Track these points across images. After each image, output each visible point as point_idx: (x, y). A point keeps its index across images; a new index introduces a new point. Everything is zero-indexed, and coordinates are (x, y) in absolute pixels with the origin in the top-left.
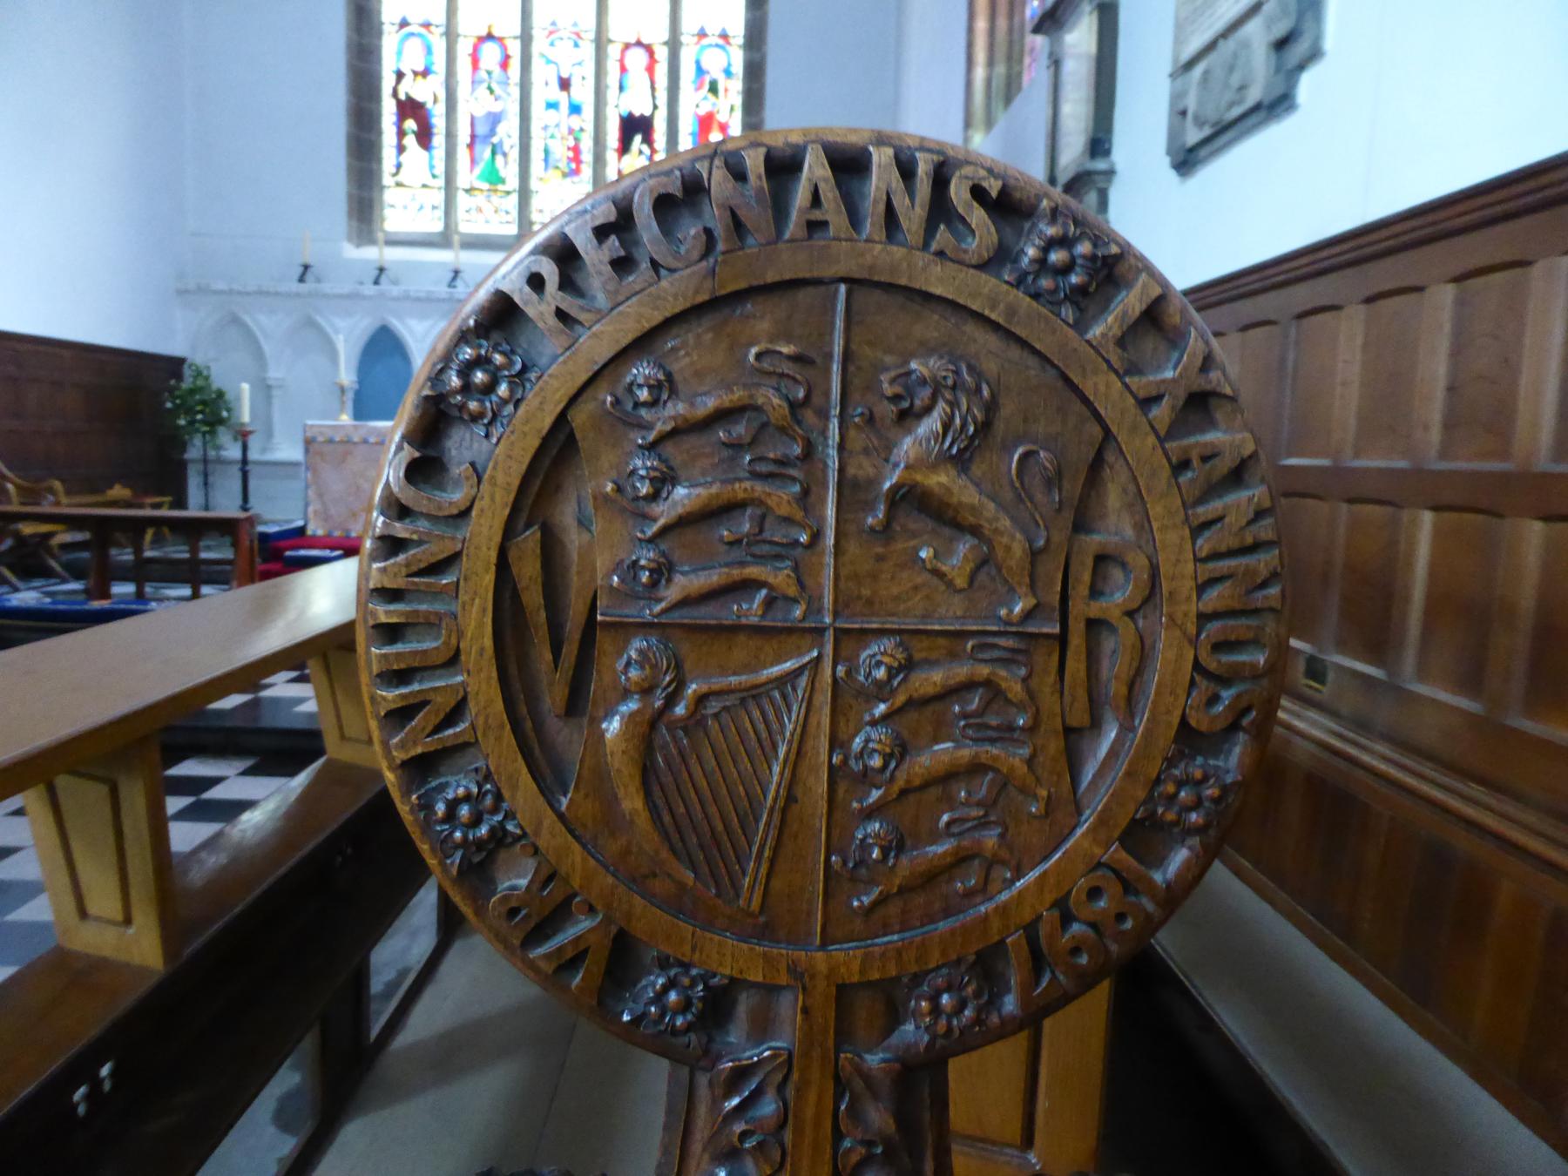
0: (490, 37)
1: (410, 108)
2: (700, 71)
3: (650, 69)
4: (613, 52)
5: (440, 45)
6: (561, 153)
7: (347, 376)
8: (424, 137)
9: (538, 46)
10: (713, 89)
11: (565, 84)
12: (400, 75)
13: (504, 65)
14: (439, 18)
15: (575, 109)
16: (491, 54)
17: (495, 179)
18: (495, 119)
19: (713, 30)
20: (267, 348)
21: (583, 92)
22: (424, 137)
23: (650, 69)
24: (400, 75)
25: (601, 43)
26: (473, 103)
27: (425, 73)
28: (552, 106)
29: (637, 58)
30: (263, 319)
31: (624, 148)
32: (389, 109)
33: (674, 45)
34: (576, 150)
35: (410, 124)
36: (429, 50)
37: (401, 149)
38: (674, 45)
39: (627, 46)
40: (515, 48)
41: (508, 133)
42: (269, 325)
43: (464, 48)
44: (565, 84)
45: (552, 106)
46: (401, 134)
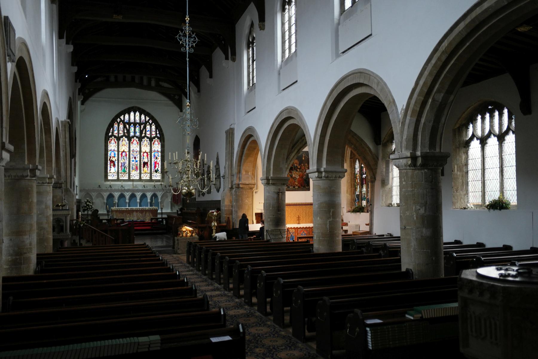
0: (124, 151)
1: (112, 162)
2: (154, 156)
3: (147, 156)
4: (142, 153)
5: (116, 153)
6: (134, 167)
7: (105, 201)
8: (114, 165)
9: (131, 152)
10: (157, 158)
11: (135, 158)
12: (110, 157)
13: (126, 155)
14: (116, 149)
15: (137, 161)
16: (124, 154)
17: (125, 171)
18: (124, 163)
19: (156, 150)
20: (93, 197)
21: (138, 159)
22: (114, 165)
23: (147, 156)
24: (110, 157)
25: (140, 151)
26: (121, 161)
27: (114, 157)
28: (133, 161)
29: (145, 154)
30: (93, 193)
31: (144, 167)
32: (109, 161)
33: (151, 152)
34: (137, 167)
35: (112, 164)
36: (115, 154)
37: (111, 167)
38: (151, 152)
39: (144, 153)
40: (128, 153)
41: (127, 165)
42: (94, 195)
43: (120, 153)
44: (135, 158)
45: (133, 161)
46: (111, 165)
